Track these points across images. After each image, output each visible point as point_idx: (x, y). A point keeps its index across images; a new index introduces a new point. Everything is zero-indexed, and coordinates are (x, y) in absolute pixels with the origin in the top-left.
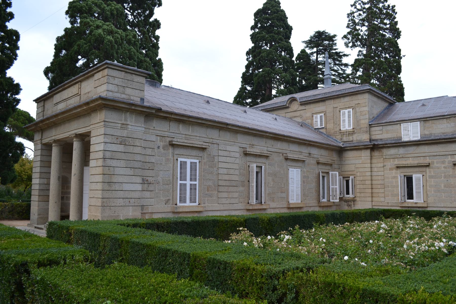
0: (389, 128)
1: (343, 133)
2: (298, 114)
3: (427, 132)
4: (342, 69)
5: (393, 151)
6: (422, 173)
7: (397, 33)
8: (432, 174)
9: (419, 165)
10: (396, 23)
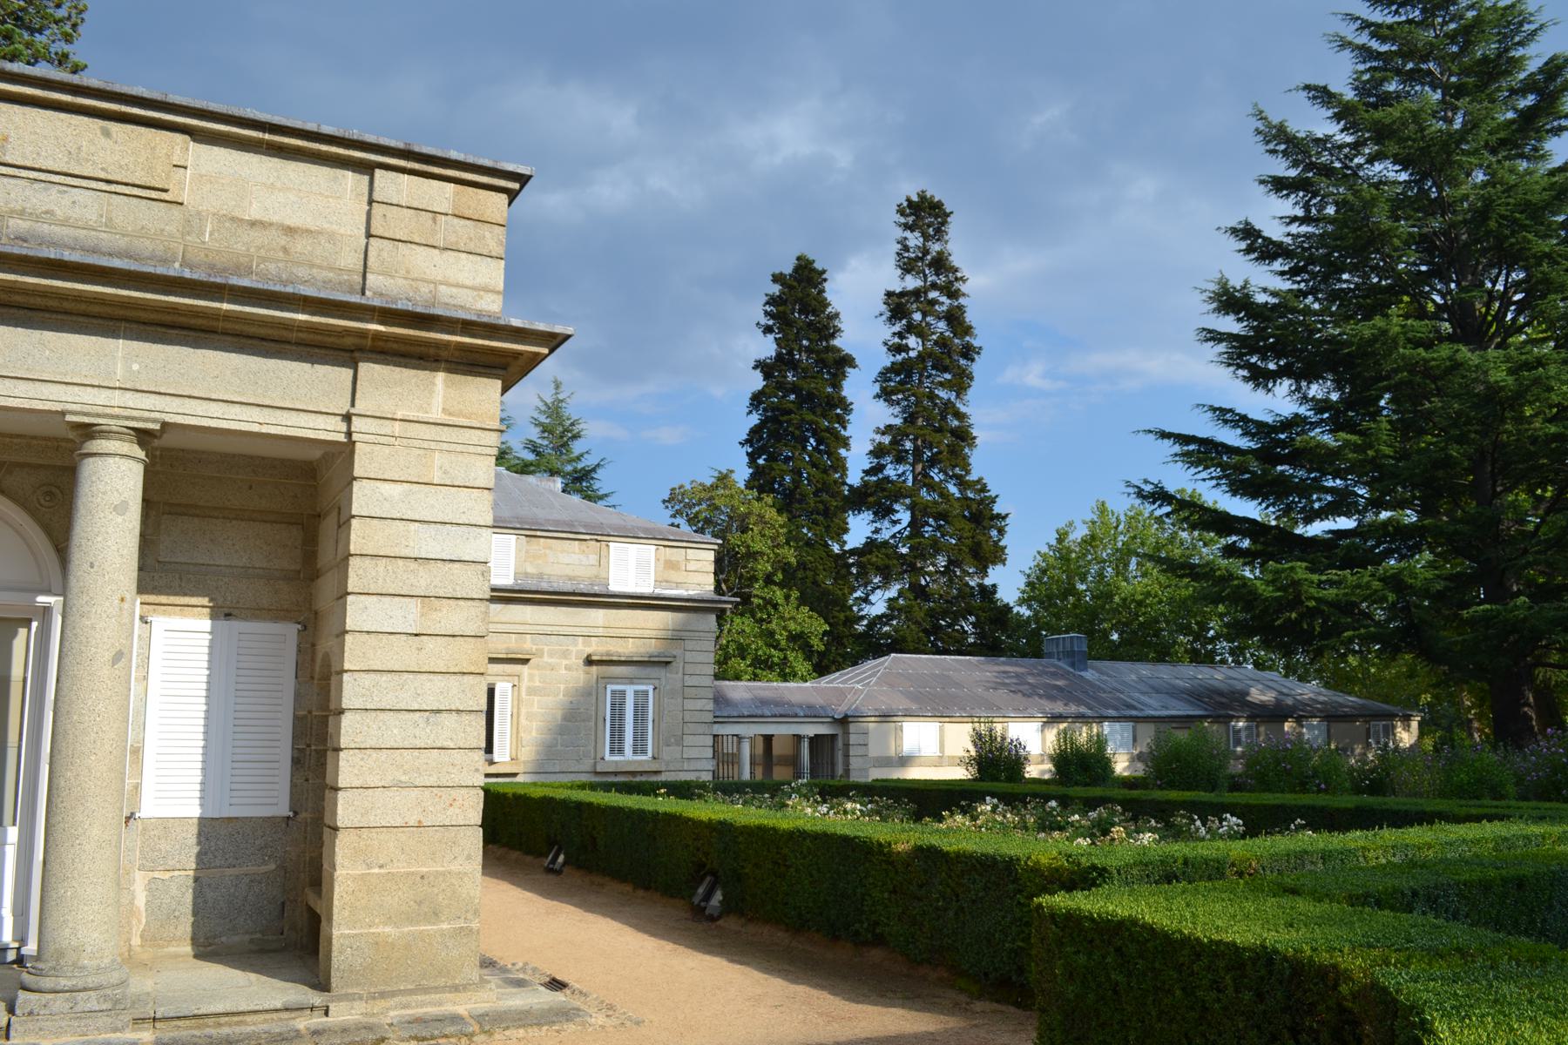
3: (531, 569)
6: (510, 678)
8: (537, 684)
9: (510, 656)
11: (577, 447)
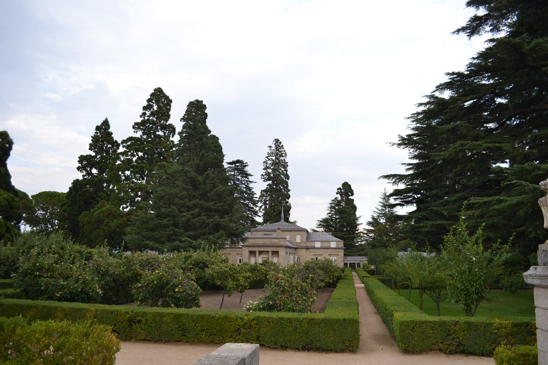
0: (312, 243)
1: (297, 243)
2: (280, 234)
3: (322, 245)
4: (247, 183)
5: (312, 250)
7: (288, 177)
10: (287, 171)
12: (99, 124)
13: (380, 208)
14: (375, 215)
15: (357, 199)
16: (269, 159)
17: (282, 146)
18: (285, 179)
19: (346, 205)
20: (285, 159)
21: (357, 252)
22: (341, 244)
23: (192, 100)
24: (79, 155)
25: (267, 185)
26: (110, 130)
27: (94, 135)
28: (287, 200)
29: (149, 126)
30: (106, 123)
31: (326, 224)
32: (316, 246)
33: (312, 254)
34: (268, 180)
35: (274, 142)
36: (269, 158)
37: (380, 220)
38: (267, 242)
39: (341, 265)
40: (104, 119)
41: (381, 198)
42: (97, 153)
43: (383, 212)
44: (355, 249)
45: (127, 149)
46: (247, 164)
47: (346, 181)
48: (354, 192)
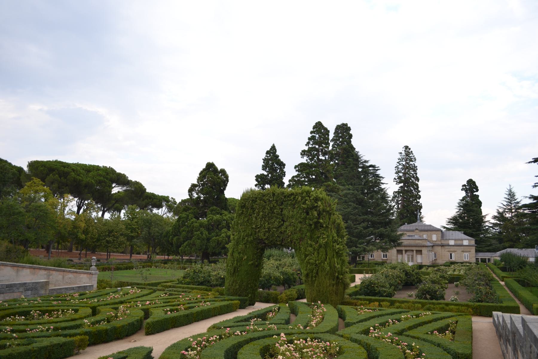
0: (446, 241)
1: (433, 241)
2: (418, 233)
3: (456, 243)
7: (418, 179)
10: (416, 174)
11: (516, 197)
12: (269, 149)
13: (505, 203)
14: (501, 210)
15: (481, 194)
16: (400, 164)
17: (412, 151)
18: (415, 181)
19: (471, 200)
20: (415, 164)
21: (485, 247)
22: (473, 242)
23: (340, 124)
24: (256, 175)
25: (399, 187)
26: (277, 153)
27: (265, 158)
28: (418, 200)
29: (314, 153)
30: (273, 148)
31: (454, 221)
32: (450, 244)
33: (446, 250)
34: (400, 183)
35: (404, 149)
36: (400, 163)
37: (506, 214)
38: (412, 242)
39: (474, 260)
40: (272, 145)
41: (506, 194)
42: (269, 172)
43: (509, 207)
44: (484, 245)
45: (299, 172)
46: (378, 168)
47: (470, 178)
48: (478, 188)
